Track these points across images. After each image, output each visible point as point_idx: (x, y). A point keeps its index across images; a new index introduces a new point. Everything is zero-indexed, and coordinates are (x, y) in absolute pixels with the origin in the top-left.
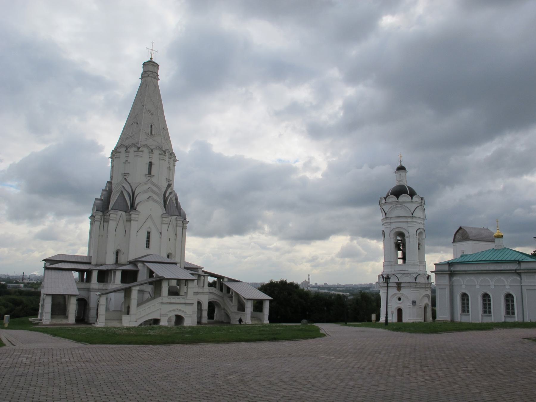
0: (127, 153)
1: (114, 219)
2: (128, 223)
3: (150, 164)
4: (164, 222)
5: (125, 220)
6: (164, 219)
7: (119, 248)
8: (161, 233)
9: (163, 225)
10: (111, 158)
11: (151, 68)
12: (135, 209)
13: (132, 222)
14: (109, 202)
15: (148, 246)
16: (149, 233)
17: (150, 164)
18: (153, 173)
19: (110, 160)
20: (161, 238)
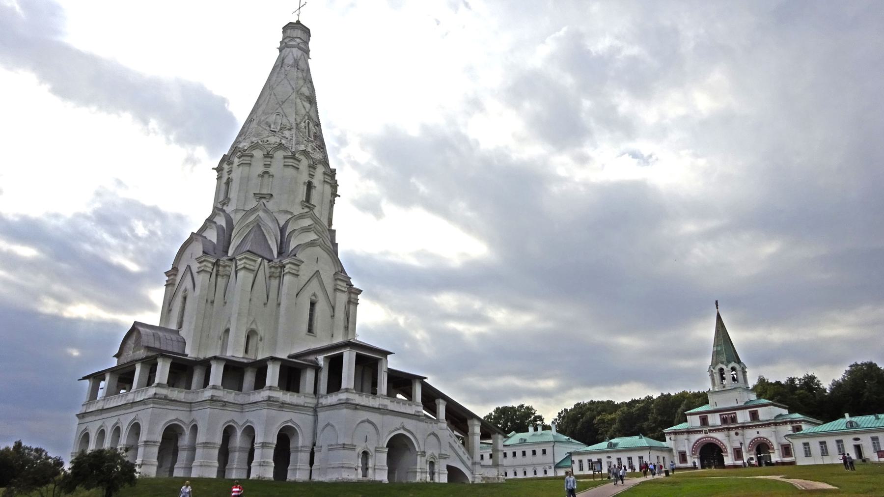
0: (269, 159)
1: (251, 267)
2: (275, 282)
3: (310, 186)
4: (339, 287)
5: (268, 275)
6: (339, 282)
7: (254, 327)
8: (333, 308)
9: (338, 294)
10: (219, 169)
11: (298, 33)
12: (295, 255)
13: (287, 278)
14: (229, 244)
15: (310, 330)
16: (313, 304)
17: (310, 186)
18: (314, 201)
19: (215, 173)
20: (333, 316)
